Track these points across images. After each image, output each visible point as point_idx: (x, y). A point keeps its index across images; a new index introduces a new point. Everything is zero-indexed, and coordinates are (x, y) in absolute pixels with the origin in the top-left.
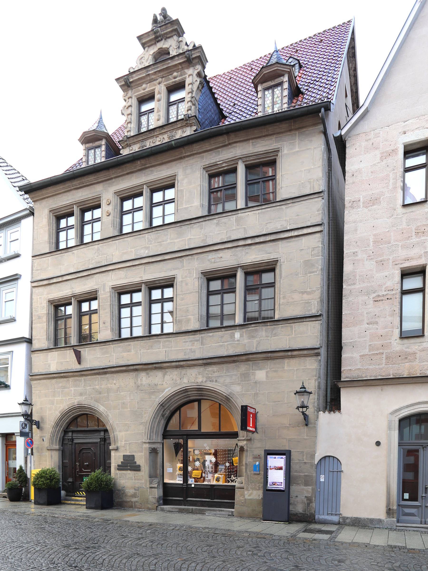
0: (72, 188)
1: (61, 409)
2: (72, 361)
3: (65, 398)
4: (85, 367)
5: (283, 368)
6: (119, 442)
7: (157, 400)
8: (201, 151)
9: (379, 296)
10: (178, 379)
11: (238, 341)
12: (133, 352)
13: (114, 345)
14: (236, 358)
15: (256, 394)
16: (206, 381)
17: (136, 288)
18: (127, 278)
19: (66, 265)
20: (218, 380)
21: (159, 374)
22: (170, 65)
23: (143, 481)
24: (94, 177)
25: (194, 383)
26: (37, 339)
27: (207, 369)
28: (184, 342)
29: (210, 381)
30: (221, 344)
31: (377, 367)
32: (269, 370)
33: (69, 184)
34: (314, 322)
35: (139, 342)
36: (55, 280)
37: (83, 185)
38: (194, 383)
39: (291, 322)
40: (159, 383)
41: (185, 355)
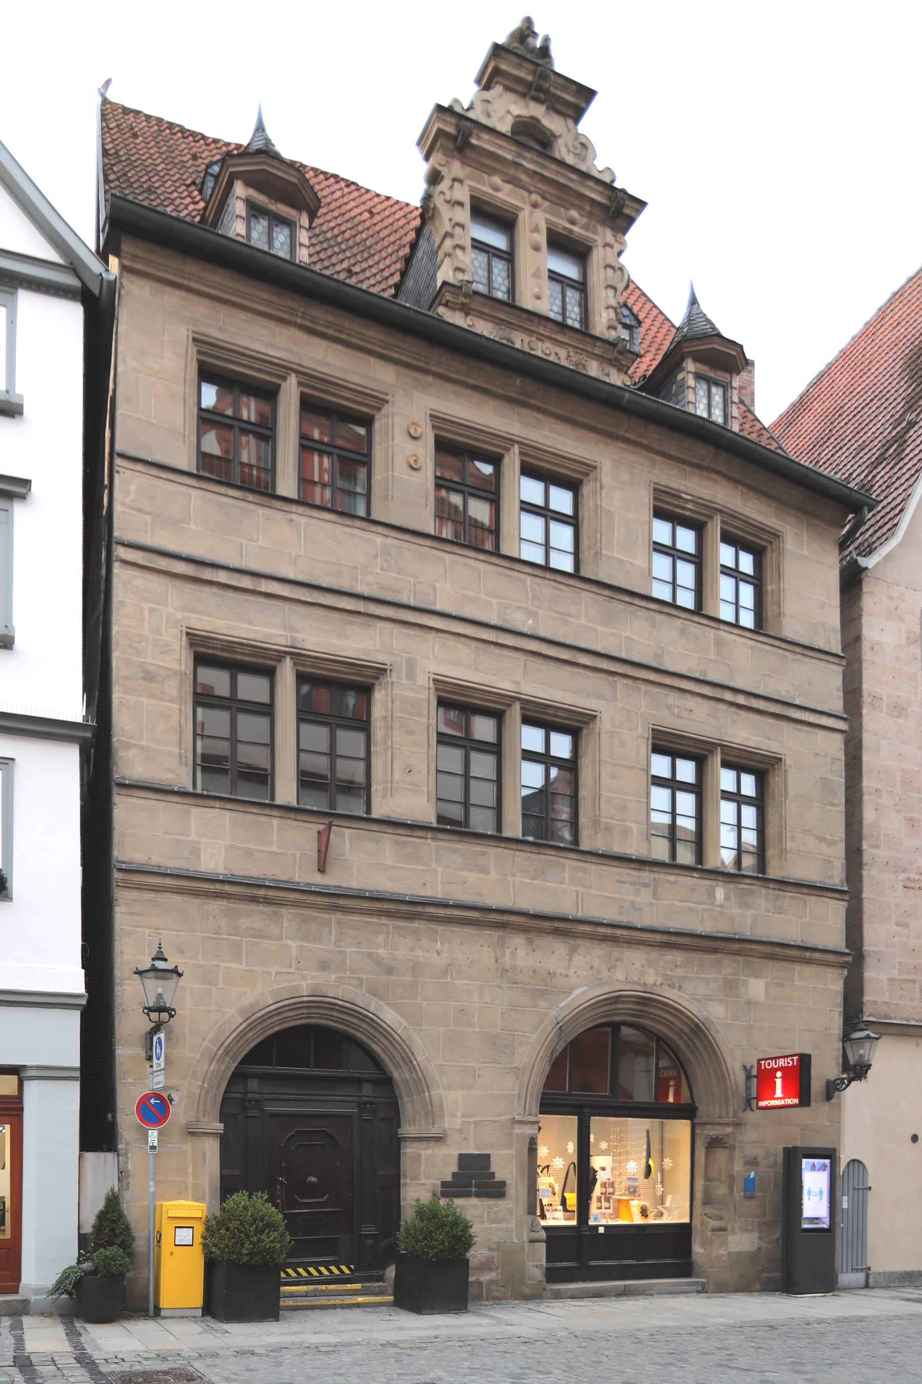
0: (299, 321)
1: (246, 1001)
2: (293, 856)
3: (261, 969)
4: (344, 885)
5: (793, 981)
6: (447, 1118)
7: (553, 1013)
8: (656, 447)
9: (909, 879)
10: (603, 968)
11: (721, 906)
12: (493, 875)
13: (440, 843)
14: (723, 945)
15: (750, 1028)
16: (661, 984)
17: (491, 705)
18: (477, 670)
19: (260, 543)
20: (684, 986)
21: (560, 947)
22: (571, 185)
23: (513, 1225)
24: (383, 338)
25: (638, 984)
26: (141, 747)
27: (664, 957)
28: (619, 882)
29: (669, 985)
30: (691, 905)
31: (909, 1003)
32: (769, 979)
33: (295, 305)
34: (838, 902)
35: (512, 852)
36: (223, 577)
37: (337, 335)
38: (638, 984)
39: (805, 891)
40: (558, 972)
41: (620, 913)
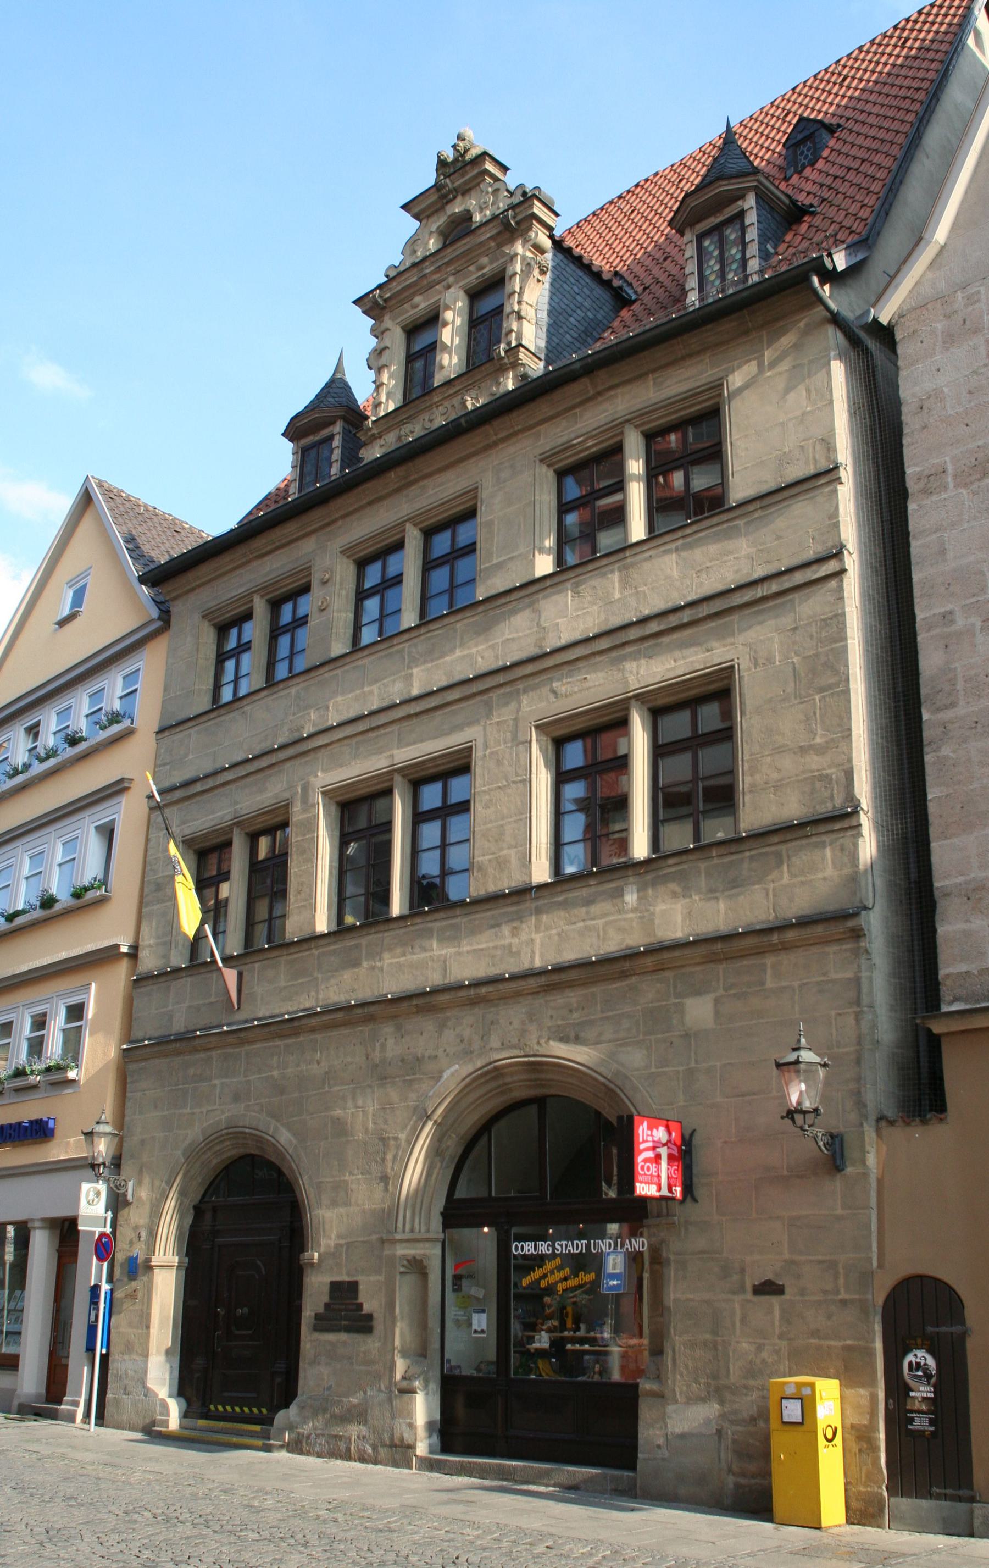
5: (762, 983)
20: (582, 1035)
21: (428, 1024)
27: (552, 1004)
32: (721, 992)
40: (427, 1054)
